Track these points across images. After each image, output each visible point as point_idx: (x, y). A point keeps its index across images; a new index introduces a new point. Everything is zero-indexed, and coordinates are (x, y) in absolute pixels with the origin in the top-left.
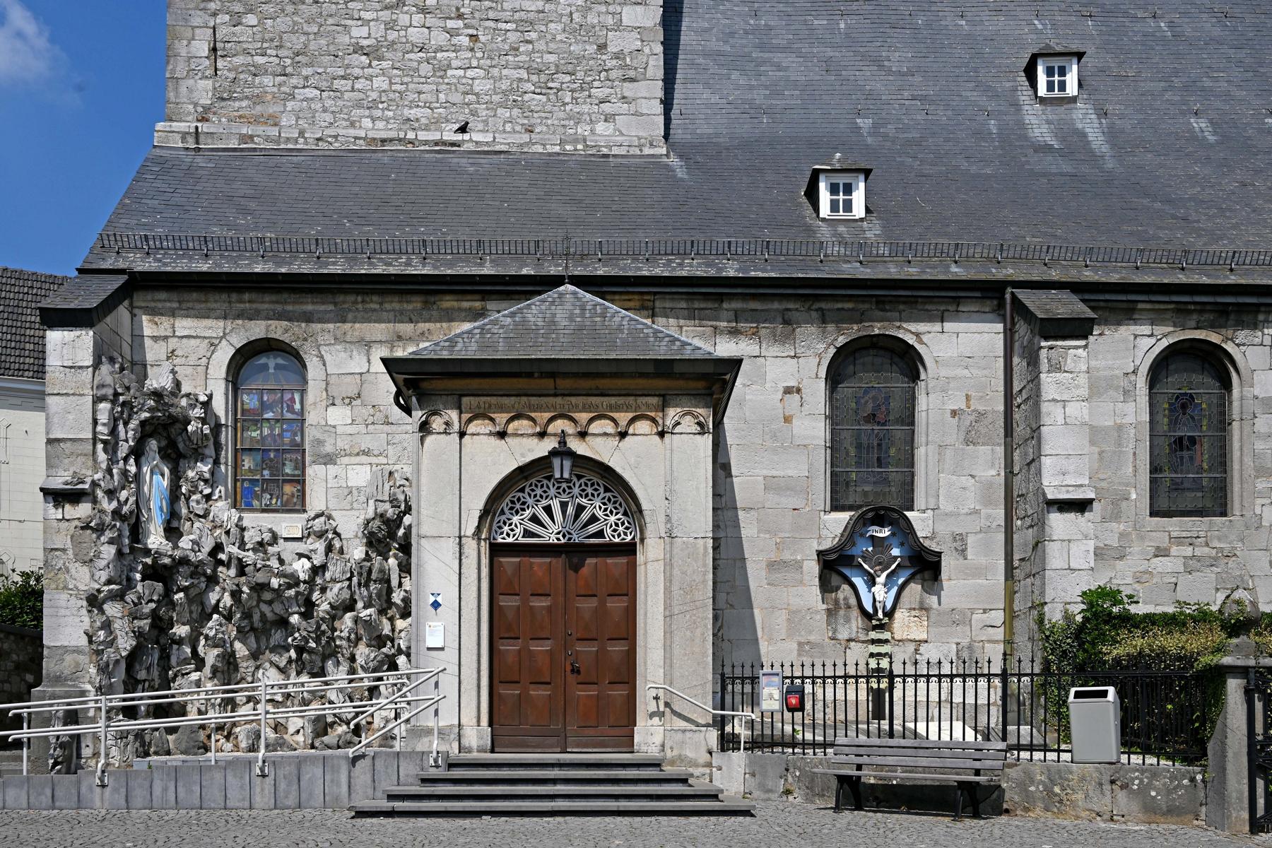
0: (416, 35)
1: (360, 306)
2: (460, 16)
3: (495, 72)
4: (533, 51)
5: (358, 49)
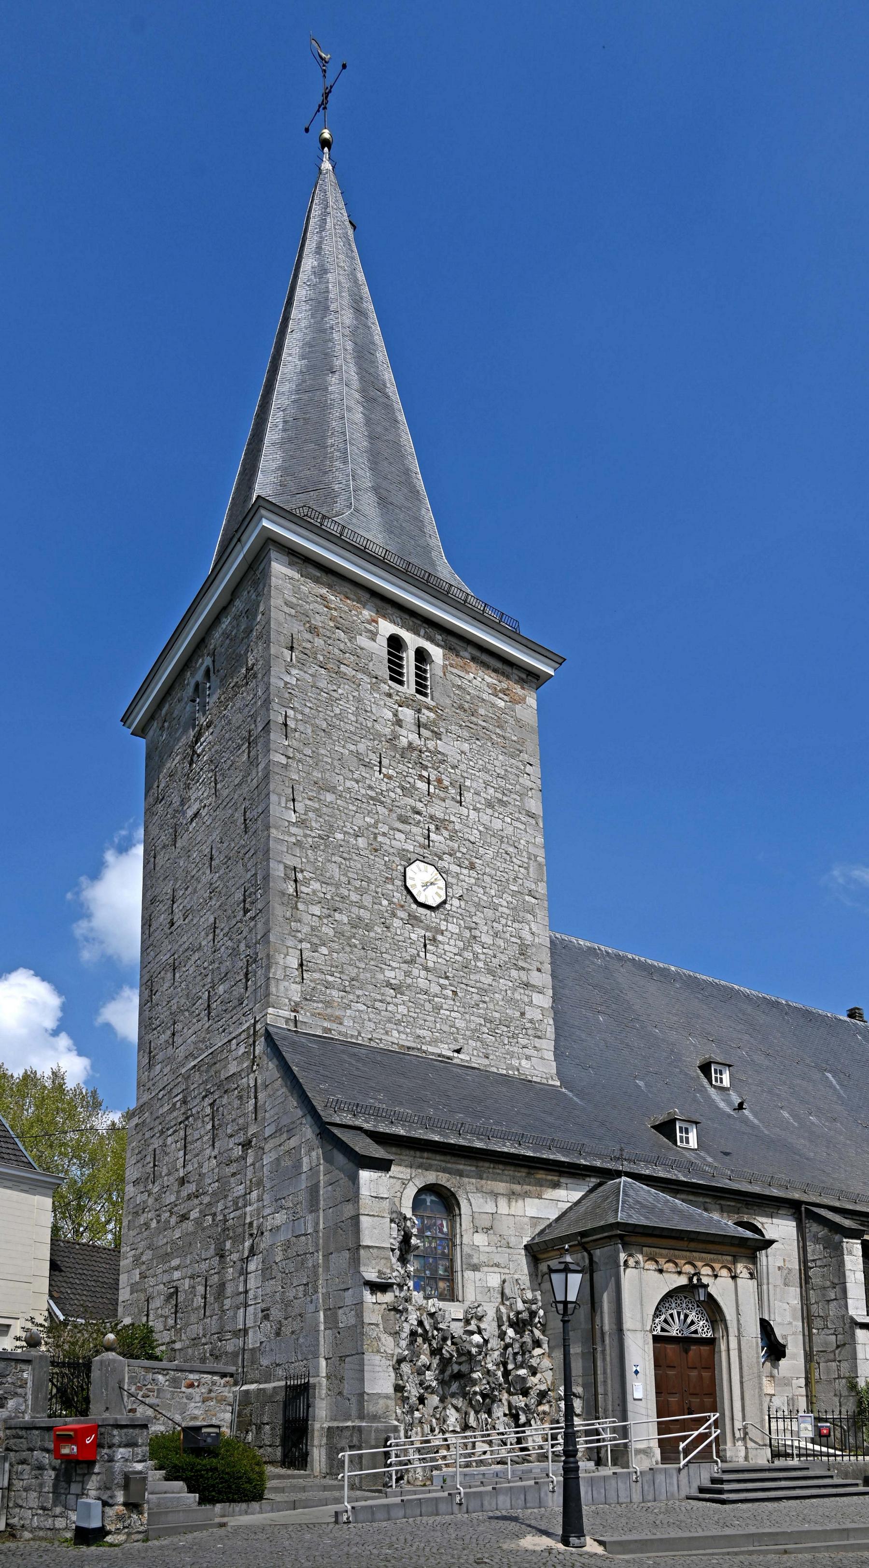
0: (422, 983)
1: (491, 1170)
2: (447, 978)
3: (467, 1016)
4: (487, 1008)
5: (389, 985)
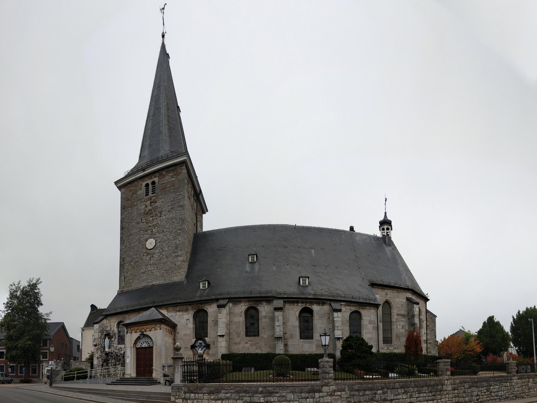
0: (149, 269)
5: (142, 273)
